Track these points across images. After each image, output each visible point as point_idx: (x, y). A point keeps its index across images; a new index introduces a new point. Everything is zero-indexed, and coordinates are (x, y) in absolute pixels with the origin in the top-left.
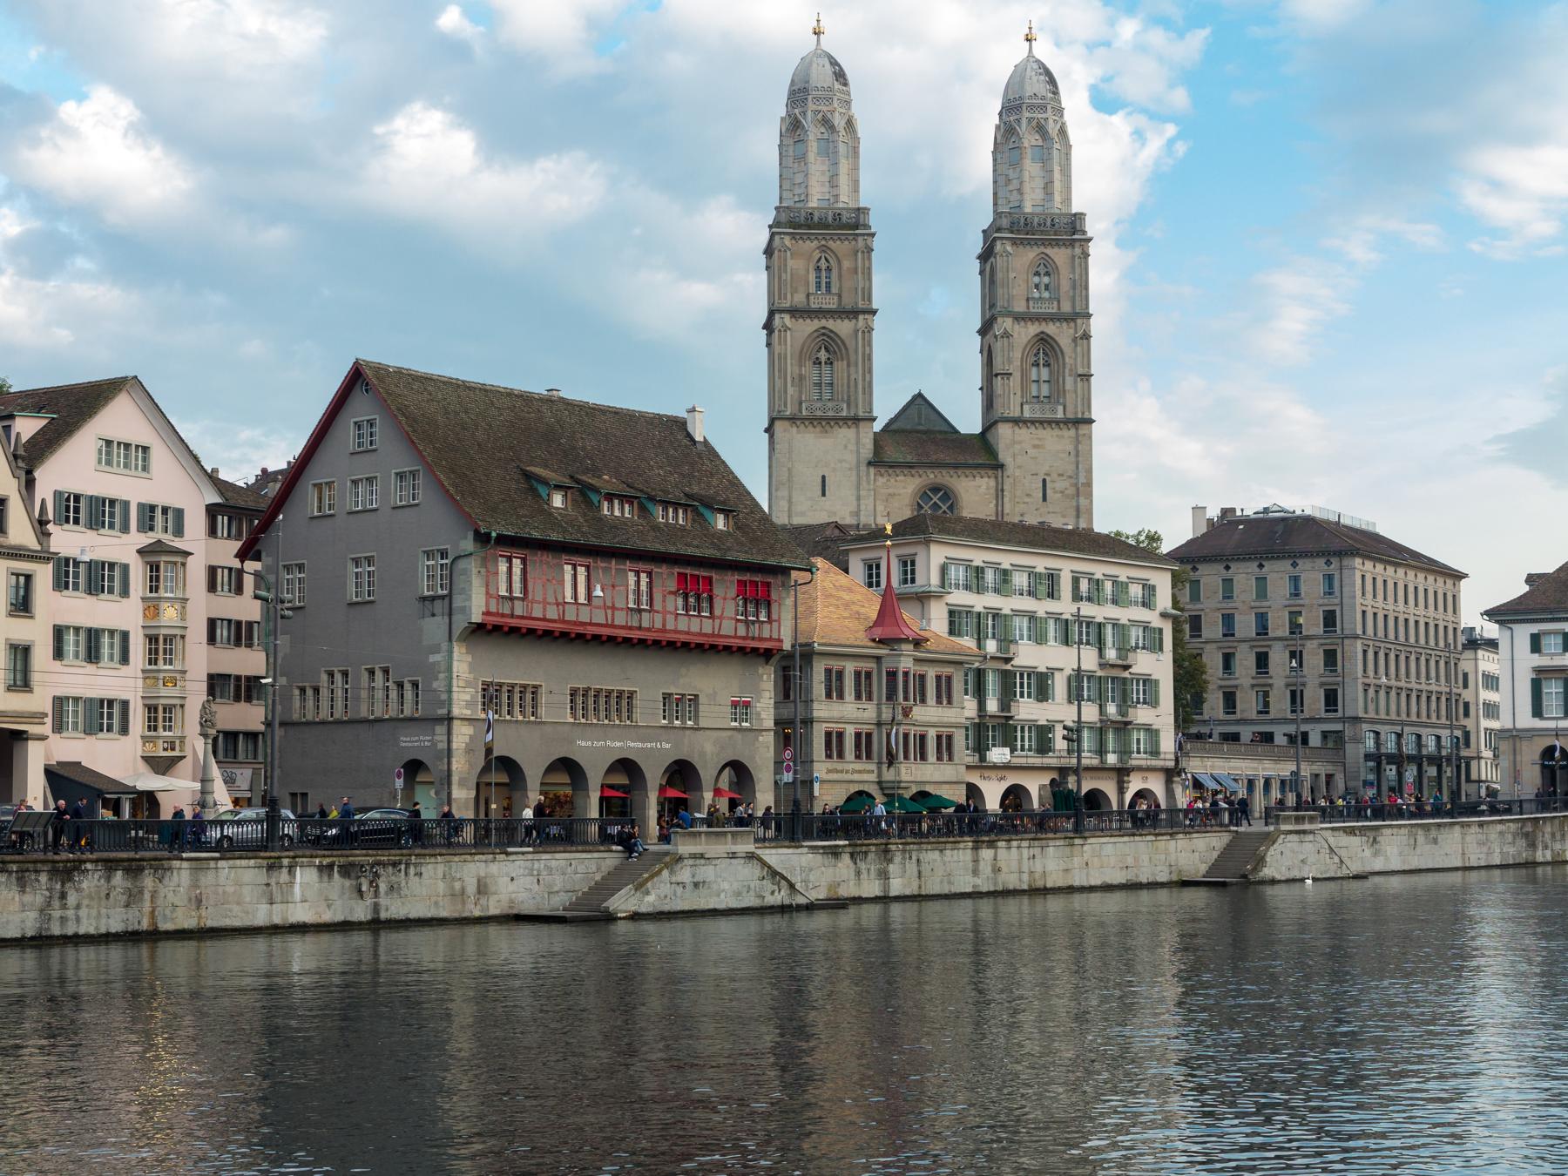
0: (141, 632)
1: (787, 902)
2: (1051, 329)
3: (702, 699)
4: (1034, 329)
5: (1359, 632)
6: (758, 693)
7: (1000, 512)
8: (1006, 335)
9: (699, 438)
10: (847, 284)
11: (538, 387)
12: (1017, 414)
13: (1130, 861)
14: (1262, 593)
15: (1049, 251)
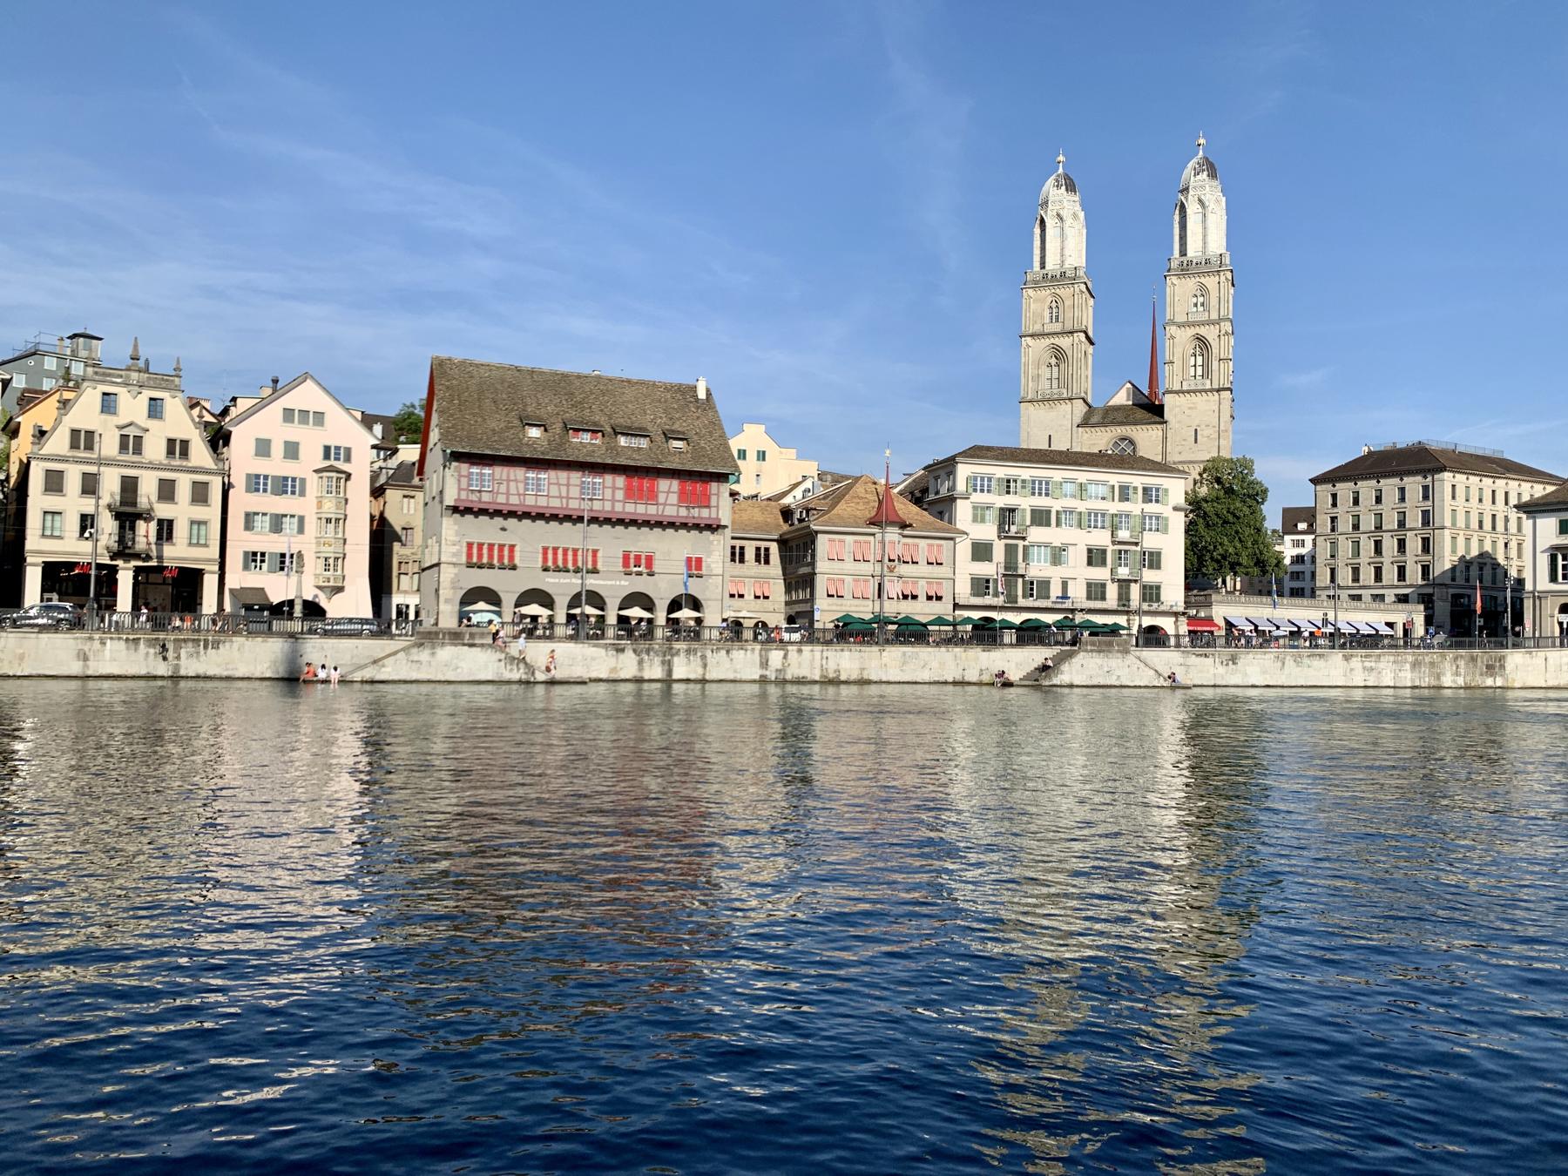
0: (315, 517)
1: (524, 677)
2: (1203, 331)
3: (657, 556)
4: (1191, 331)
5: (1448, 523)
6: (709, 554)
7: (1164, 453)
8: (1172, 337)
9: (702, 395)
10: (1069, 315)
11: (585, 370)
12: (1177, 387)
13: (935, 664)
14: (1379, 500)
15: (1202, 280)
